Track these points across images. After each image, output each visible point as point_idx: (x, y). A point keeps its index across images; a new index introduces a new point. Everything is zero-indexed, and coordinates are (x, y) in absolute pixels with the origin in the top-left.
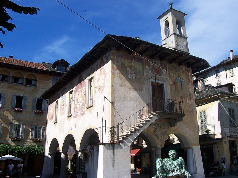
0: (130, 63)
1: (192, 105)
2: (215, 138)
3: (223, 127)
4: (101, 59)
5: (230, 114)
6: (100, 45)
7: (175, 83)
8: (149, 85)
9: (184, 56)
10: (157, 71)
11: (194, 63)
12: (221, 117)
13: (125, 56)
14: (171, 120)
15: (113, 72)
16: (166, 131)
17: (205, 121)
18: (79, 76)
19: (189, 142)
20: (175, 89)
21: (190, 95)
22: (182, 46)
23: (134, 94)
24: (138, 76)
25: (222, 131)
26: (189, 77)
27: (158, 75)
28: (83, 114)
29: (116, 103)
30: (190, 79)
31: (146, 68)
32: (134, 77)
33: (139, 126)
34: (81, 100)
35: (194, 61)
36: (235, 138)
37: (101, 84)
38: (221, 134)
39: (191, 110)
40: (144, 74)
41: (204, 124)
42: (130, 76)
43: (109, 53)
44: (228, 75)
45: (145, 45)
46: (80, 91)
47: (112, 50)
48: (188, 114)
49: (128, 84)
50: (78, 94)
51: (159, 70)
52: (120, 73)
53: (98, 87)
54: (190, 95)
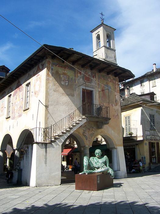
0: (64, 71)
1: (118, 110)
2: (138, 140)
3: (144, 130)
4: (37, 66)
5: (151, 119)
6: (37, 54)
7: (103, 90)
9: (112, 66)
10: (87, 80)
11: (121, 74)
12: (143, 122)
14: (98, 123)
15: (48, 79)
16: (93, 132)
17: (129, 125)
18: (18, 81)
19: (114, 142)
21: (116, 101)
22: (111, 58)
23: (66, 99)
25: (143, 134)
27: (88, 83)
28: (20, 116)
30: (117, 87)
31: (78, 76)
32: (67, 84)
33: (69, 128)
34: (19, 103)
35: (120, 71)
36: (154, 140)
37: (37, 89)
38: (143, 136)
39: (116, 114)
40: (75, 82)
41: (128, 128)
42: (63, 83)
43: (44, 61)
44: (151, 86)
45: (77, 55)
46: (18, 95)
47: (47, 58)
48: (114, 118)
49: (61, 90)
50: (16, 98)
52: (54, 80)
53: (34, 92)
54: (116, 101)
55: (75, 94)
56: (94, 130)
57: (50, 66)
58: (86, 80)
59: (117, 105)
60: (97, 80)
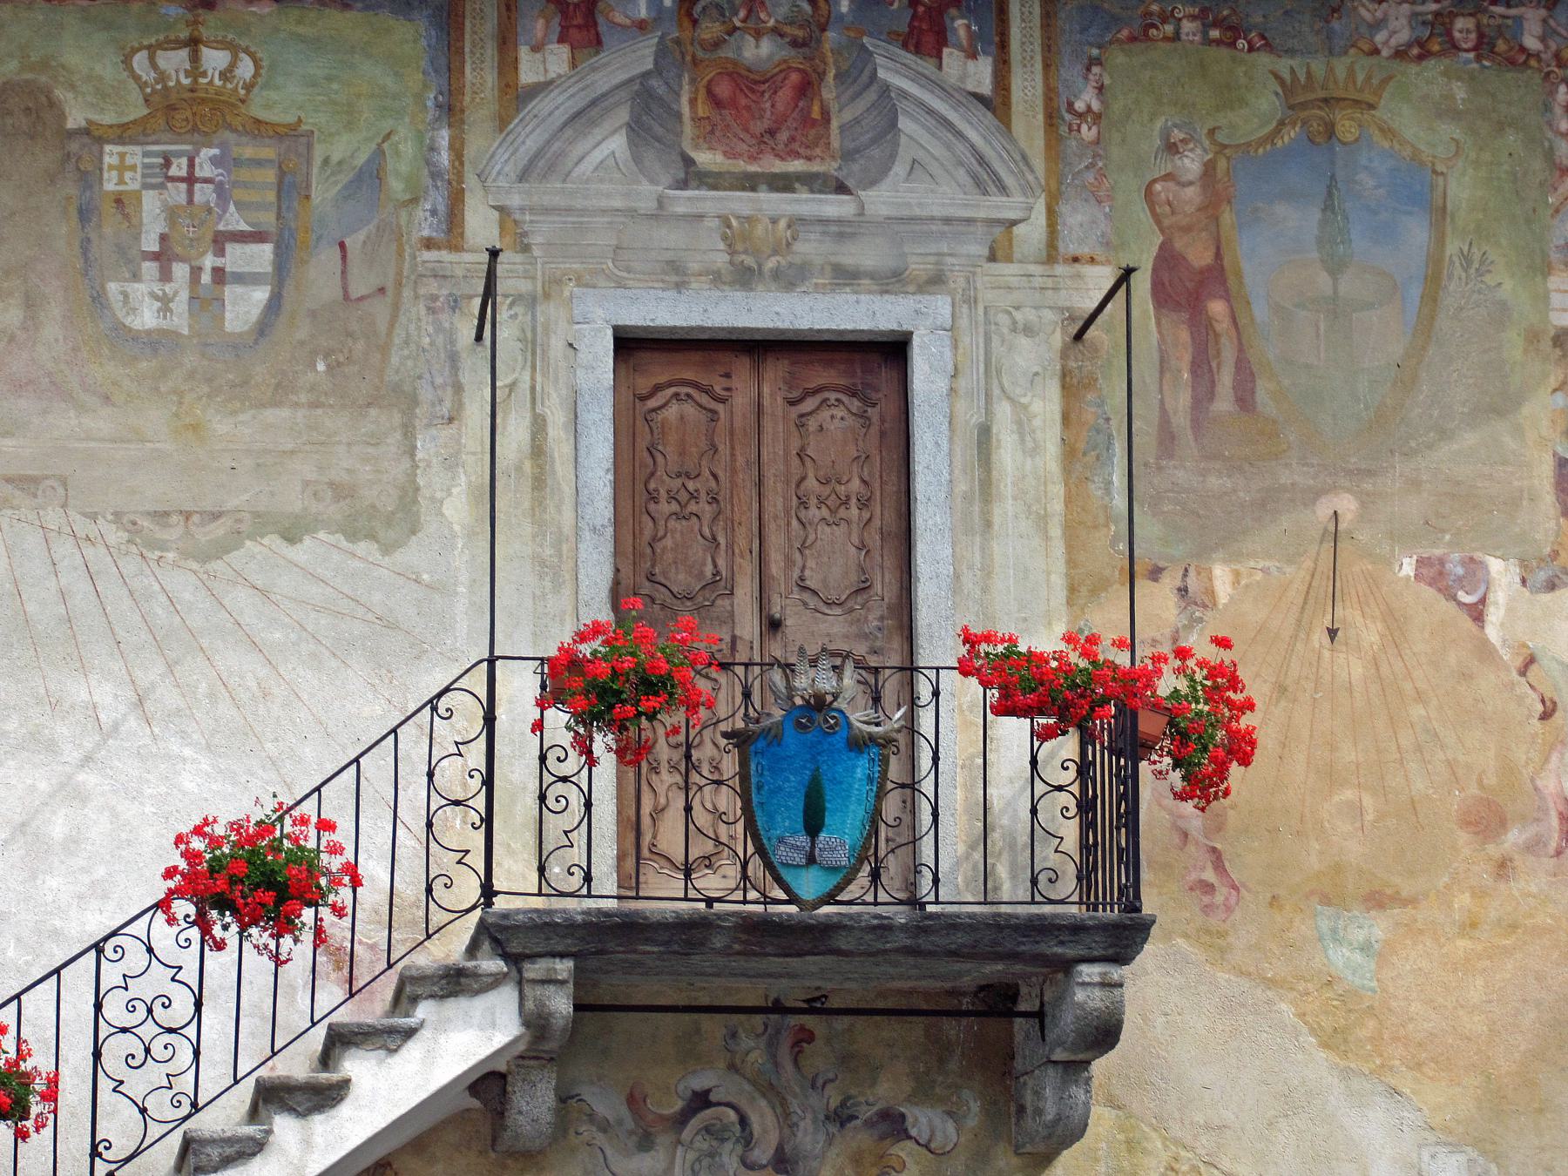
0: (174, 61)
8: (557, 419)
20: (1181, 401)
24: (320, 277)
27: (783, 183)
32: (244, 306)
42: (144, 305)
51: (807, 88)
55: (431, 480)
58: (709, 133)
60: (1027, 87)
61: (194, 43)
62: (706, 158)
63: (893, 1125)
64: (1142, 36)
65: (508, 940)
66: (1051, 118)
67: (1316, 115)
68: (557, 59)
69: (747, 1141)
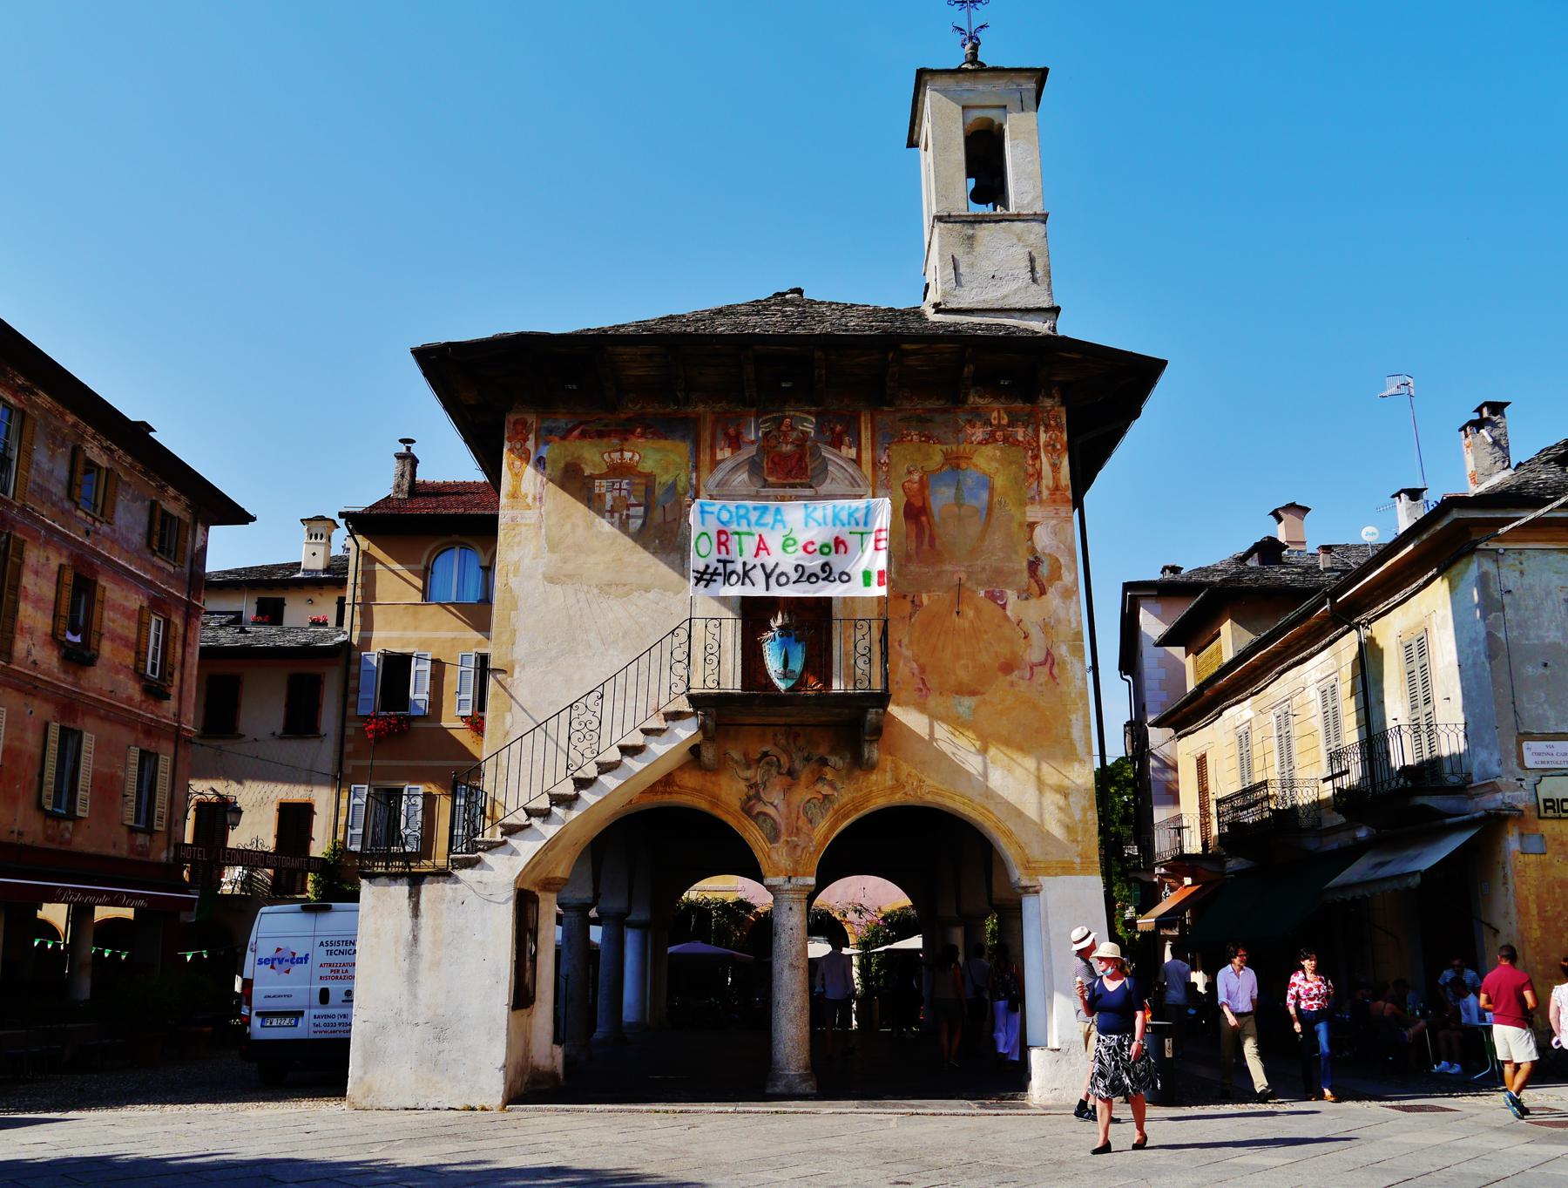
0: (616, 456)
13: (586, 423)
16: (826, 790)
17: (1427, 701)
21: (1034, 566)
24: (657, 516)
26: (1036, 457)
29: (517, 670)
39: (1036, 655)
41: (1423, 721)
51: (801, 458)
54: (1034, 566)
56: (829, 777)
57: (530, 444)
58: (771, 473)
59: (1043, 592)
60: (866, 456)
61: (622, 451)
62: (770, 479)
63: (823, 762)
64: (901, 441)
65: (696, 701)
66: (874, 465)
67: (954, 463)
68: (727, 453)
69: (779, 766)
